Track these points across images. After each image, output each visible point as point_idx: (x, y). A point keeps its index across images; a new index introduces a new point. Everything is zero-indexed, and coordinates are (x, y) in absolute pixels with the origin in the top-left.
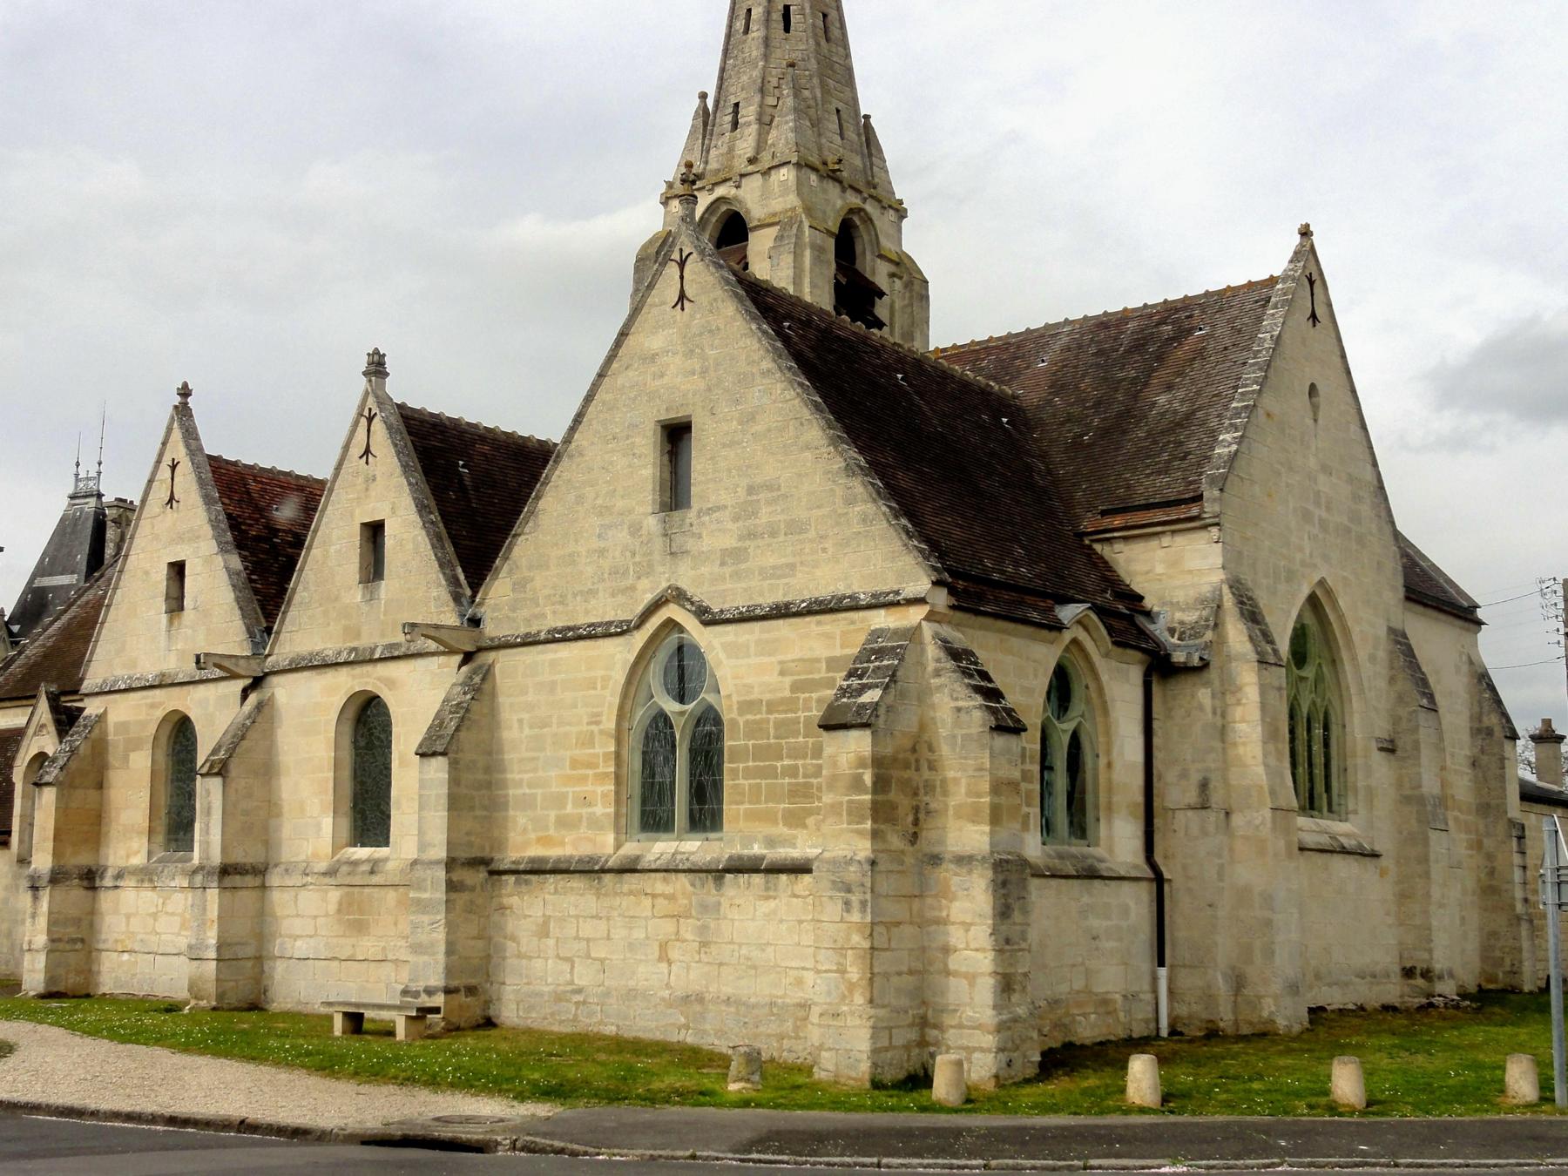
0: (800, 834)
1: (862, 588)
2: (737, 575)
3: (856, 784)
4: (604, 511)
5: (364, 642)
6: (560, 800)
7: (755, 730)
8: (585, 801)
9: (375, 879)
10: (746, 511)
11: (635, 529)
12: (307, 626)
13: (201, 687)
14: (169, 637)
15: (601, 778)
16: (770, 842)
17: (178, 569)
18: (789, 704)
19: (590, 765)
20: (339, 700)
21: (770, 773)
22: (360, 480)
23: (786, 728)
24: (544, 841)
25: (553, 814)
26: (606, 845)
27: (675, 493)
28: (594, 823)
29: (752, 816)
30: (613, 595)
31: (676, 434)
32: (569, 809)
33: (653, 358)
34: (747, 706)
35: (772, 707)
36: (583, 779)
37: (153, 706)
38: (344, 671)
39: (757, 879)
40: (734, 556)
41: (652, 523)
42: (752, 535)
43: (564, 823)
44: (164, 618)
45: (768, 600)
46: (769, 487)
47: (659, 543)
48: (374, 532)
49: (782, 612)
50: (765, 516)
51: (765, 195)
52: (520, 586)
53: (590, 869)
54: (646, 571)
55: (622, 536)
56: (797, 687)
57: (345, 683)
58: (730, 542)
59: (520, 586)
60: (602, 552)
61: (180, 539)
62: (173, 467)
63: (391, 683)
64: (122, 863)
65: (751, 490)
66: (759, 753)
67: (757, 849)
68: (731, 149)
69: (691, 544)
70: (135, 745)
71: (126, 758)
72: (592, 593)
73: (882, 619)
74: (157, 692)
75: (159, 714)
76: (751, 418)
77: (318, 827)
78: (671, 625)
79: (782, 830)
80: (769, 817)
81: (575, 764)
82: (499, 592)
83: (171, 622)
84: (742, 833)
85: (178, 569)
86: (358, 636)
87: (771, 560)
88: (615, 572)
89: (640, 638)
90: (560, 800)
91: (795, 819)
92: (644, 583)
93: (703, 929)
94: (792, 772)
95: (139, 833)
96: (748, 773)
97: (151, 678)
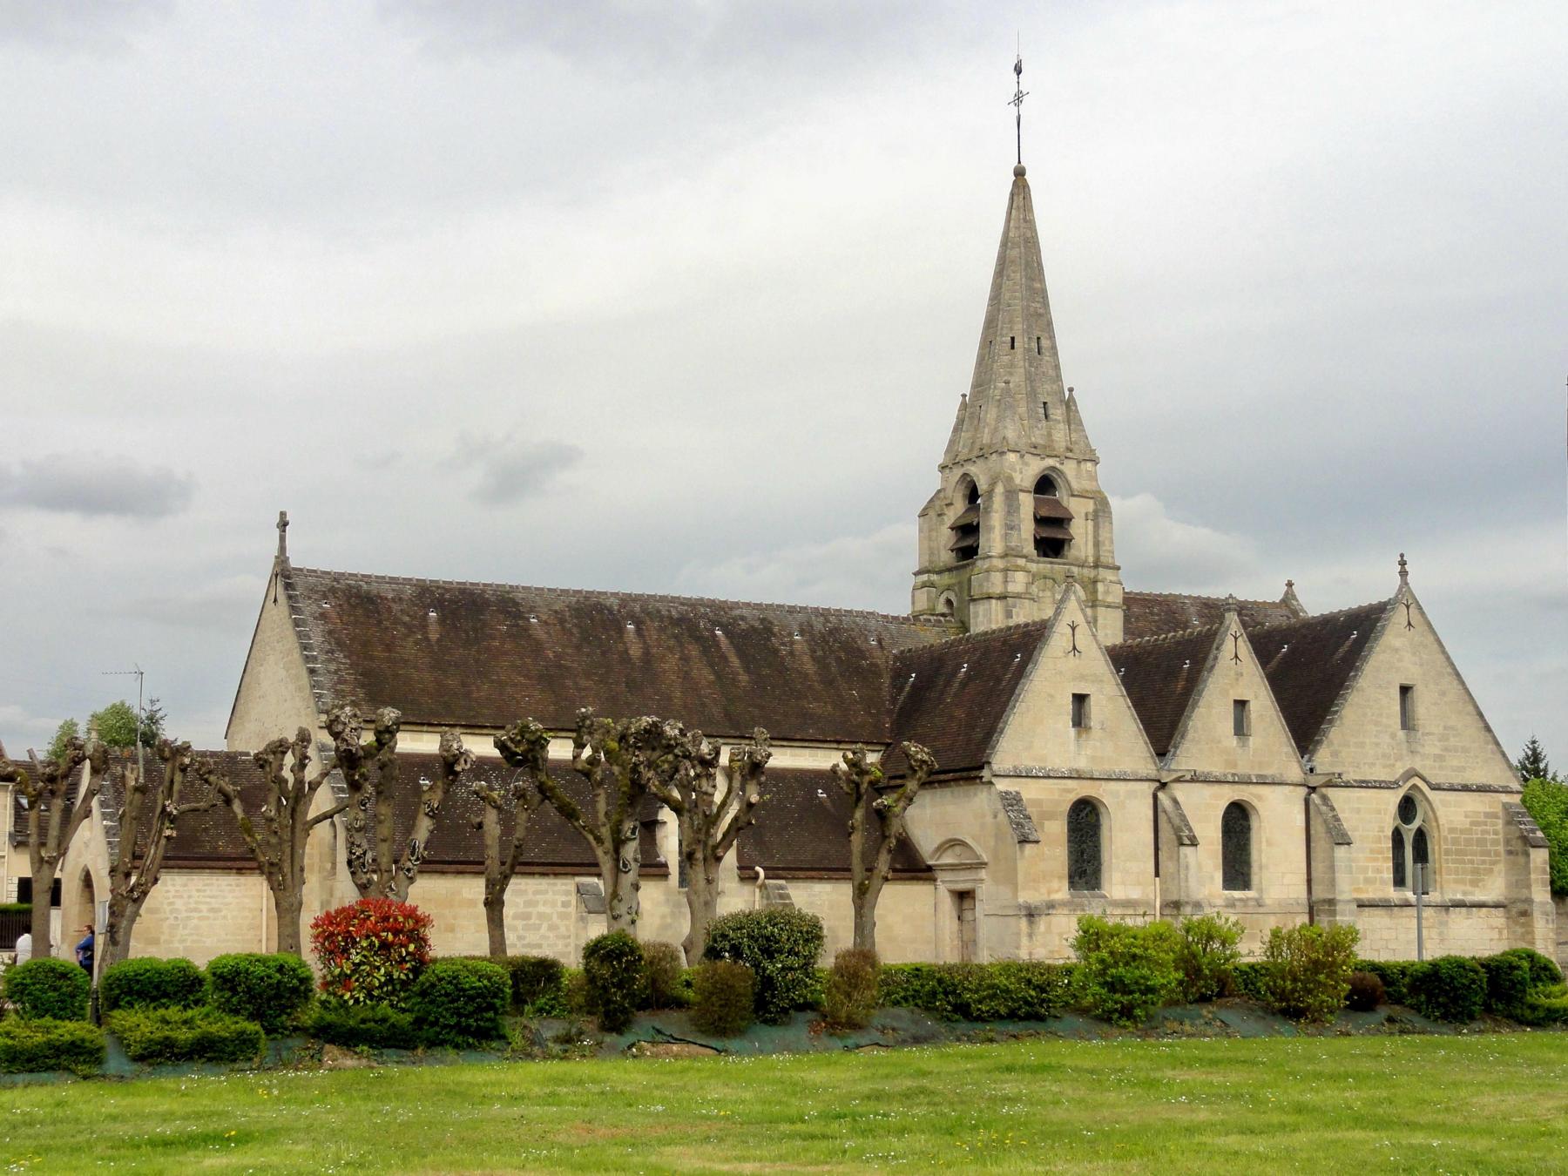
0: (1477, 891)
1: (1495, 783)
2: (1441, 768)
3: (1544, 872)
4: (1377, 723)
5: (1243, 769)
6: (1365, 870)
7: (1455, 841)
8: (1378, 871)
9: (1261, 910)
10: (1443, 738)
11: (1393, 736)
12: (1191, 754)
13: (1112, 784)
14: (1079, 746)
15: (1385, 859)
16: (1465, 893)
17: (1080, 699)
18: (1469, 831)
19: (1381, 852)
20: (1223, 805)
21: (1463, 862)
22: (1232, 673)
23: (1468, 842)
24: (1358, 890)
25: (1361, 877)
26: (1393, 894)
27: (1407, 722)
28: (1383, 882)
29: (1456, 881)
30: (1385, 766)
31: (1405, 690)
32: (1370, 874)
33: (1397, 650)
34: (1451, 830)
35: (1462, 831)
36: (1376, 860)
37: (1069, 791)
38: (1227, 786)
39: (1464, 910)
40: (1439, 758)
41: (1401, 734)
42: (1446, 749)
43: (1367, 881)
44: (1072, 731)
45: (1457, 780)
46: (1452, 728)
47: (1405, 746)
48: (1241, 705)
49: (1466, 788)
50: (1453, 741)
51: (1079, 476)
52: (1335, 754)
53: (1385, 905)
54: (1399, 758)
55: (1387, 739)
56: (1472, 823)
57: (1228, 794)
58: (1437, 751)
59: (1335, 754)
60: (1377, 745)
61: (1083, 678)
62: (1073, 629)
63: (1260, 798)
64: (1045, 897)
65: (1445, 728)
66: (1458, 852)
67: (1459, 897)
68: (1050, 435)
69: (1420, 749)
70: (1051, 816)
71: (1042, 825)
72: (1373, 764)
73: (1505, 798)
74: (1069, 782)
75: (1073, 797)
76: (1443, 694)
77: (1212, 878)
78: (1414, 786)
79: (1468, 888)
80: (1463, 882)
81: (1372, 851)
82: (1323, 759)
83: (1079, 735)
84: (1449, 887)
85: (1080, 699)
86: (1235, 766)
87: (1455, 763)
88: (1384, 756)
89: (1401, 793)
90: (1365, 870)
91: (1474, 883)
92: (1399, 764)
93: (1440, 934)
94: (1472, 862)
95: (1060, 878)
96: (1454, 861)
97: (1065, 770)
